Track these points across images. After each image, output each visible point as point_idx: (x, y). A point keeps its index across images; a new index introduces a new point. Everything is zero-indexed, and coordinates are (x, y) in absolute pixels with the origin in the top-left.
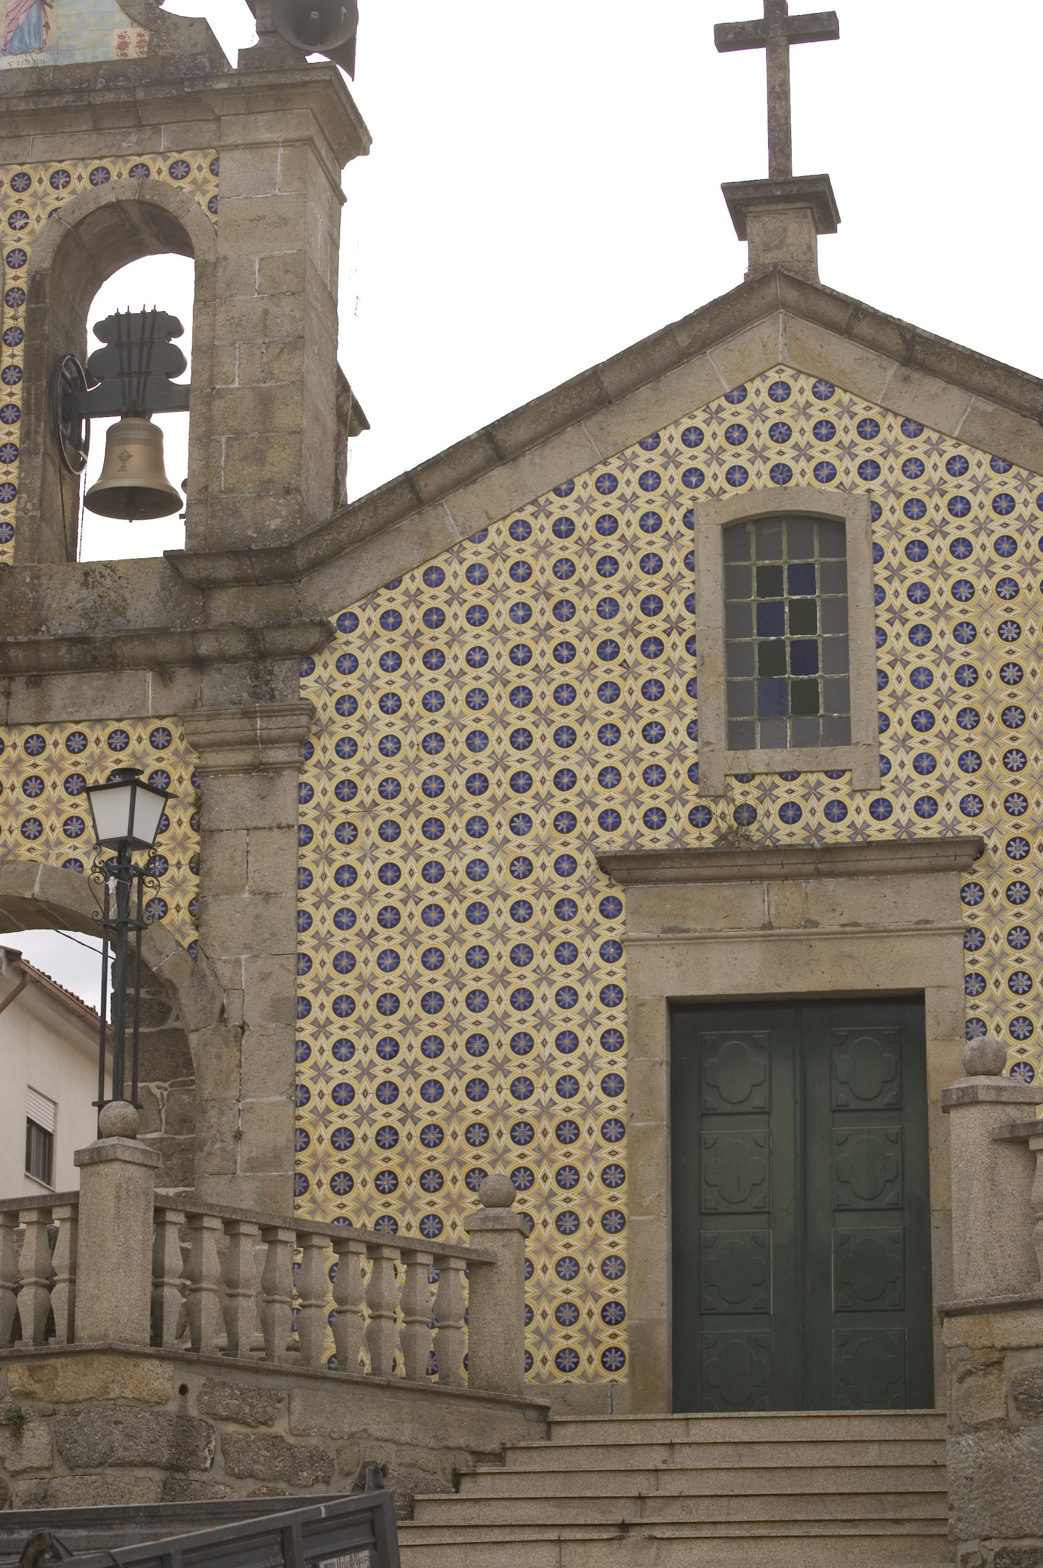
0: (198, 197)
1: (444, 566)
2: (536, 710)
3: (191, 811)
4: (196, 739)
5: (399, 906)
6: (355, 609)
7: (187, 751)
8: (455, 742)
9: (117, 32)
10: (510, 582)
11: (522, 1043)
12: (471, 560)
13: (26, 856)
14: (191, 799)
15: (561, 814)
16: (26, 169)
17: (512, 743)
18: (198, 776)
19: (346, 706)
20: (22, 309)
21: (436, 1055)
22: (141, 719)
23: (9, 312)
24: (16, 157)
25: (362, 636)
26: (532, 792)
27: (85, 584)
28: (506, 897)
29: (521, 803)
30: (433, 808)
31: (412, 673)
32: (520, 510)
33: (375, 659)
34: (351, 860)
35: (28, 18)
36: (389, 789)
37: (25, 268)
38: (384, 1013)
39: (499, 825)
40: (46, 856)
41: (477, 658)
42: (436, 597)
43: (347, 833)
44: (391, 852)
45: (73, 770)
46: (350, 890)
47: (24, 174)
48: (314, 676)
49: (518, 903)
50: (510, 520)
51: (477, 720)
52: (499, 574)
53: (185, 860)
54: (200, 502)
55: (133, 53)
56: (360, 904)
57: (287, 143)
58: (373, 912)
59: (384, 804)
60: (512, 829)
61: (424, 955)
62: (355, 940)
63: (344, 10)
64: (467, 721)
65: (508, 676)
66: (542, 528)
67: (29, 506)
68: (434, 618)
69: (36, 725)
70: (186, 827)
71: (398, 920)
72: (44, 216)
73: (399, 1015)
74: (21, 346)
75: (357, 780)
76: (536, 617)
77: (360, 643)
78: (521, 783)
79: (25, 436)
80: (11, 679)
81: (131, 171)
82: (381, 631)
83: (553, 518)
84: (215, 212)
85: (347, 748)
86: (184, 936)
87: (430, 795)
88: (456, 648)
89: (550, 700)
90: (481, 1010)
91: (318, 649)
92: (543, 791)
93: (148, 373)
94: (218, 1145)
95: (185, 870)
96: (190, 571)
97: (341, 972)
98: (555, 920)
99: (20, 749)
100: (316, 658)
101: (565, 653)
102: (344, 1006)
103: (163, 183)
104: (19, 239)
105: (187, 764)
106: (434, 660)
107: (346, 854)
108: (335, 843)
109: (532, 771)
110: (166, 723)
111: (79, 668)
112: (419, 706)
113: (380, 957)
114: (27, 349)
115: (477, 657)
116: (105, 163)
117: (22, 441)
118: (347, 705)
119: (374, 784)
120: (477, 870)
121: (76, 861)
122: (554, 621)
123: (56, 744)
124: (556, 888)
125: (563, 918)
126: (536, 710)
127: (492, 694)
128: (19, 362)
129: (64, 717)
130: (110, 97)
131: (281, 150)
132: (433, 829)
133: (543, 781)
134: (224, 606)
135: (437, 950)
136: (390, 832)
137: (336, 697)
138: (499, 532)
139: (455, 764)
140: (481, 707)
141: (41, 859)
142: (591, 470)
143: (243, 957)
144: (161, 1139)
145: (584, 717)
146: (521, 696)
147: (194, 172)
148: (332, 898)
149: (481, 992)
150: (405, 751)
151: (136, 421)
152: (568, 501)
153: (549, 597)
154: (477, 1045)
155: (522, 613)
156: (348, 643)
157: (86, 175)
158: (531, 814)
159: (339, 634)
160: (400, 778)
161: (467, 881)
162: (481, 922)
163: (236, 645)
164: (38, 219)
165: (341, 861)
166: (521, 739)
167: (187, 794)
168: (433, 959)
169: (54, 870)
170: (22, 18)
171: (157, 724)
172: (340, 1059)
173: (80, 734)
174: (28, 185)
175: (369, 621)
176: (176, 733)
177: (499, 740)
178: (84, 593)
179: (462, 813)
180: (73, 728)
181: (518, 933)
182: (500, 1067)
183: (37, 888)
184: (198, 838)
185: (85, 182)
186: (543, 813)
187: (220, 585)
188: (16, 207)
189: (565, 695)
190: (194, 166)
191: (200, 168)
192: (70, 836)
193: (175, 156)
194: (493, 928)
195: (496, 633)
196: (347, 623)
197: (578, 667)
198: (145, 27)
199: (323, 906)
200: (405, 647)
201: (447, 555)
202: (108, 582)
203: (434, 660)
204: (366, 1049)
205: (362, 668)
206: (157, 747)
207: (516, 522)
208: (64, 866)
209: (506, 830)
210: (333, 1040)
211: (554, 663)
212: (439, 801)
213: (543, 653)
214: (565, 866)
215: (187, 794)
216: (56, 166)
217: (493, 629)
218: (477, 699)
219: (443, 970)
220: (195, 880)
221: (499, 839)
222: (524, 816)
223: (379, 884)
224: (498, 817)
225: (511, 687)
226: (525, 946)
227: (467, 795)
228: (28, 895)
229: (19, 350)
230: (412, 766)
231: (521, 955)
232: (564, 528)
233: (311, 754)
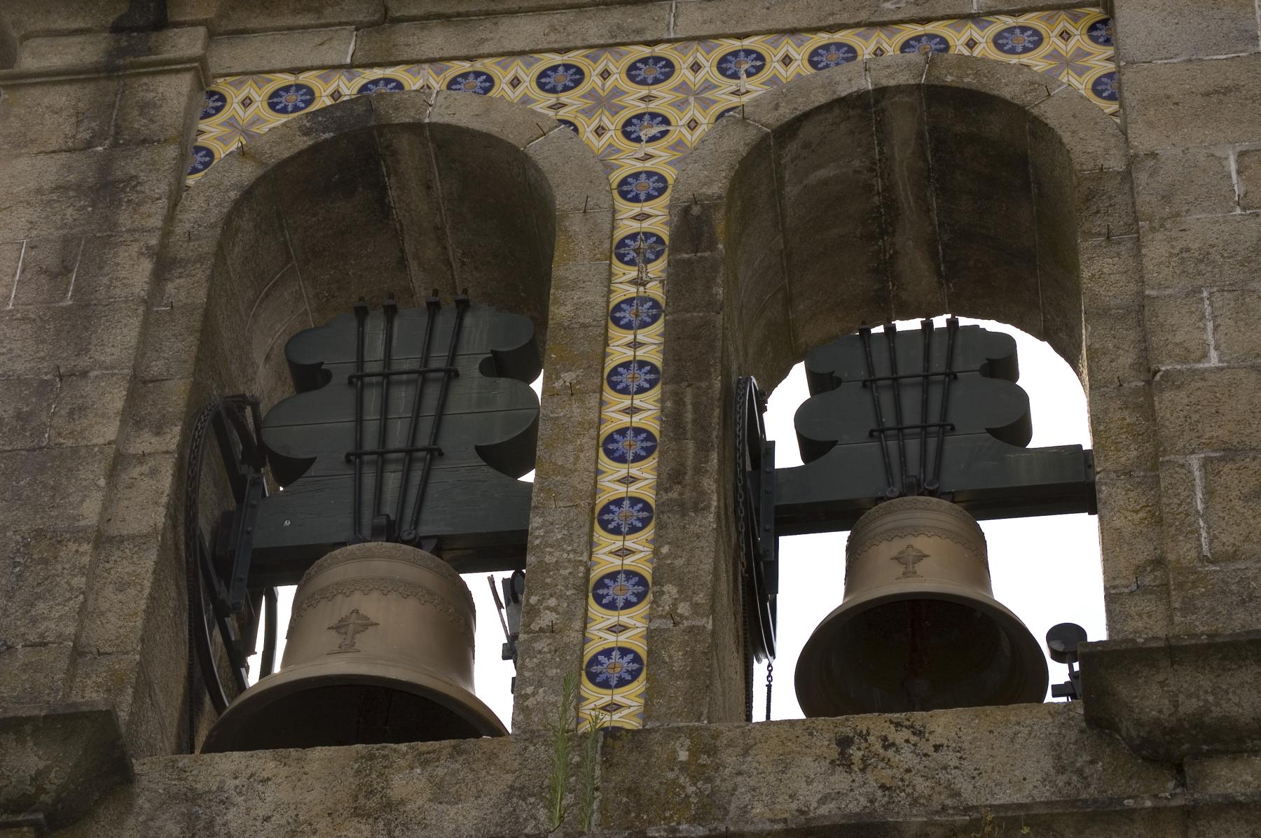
20: (657, 268)
37: (665, 199)
54: (1142, 590)
67: (683, 609)
74: (659, 326)
79: (670, 478)
93: (946, 428)
96: (1150, 699)
103: (984, 60)
178: (840, 780)
202: (906, 757)
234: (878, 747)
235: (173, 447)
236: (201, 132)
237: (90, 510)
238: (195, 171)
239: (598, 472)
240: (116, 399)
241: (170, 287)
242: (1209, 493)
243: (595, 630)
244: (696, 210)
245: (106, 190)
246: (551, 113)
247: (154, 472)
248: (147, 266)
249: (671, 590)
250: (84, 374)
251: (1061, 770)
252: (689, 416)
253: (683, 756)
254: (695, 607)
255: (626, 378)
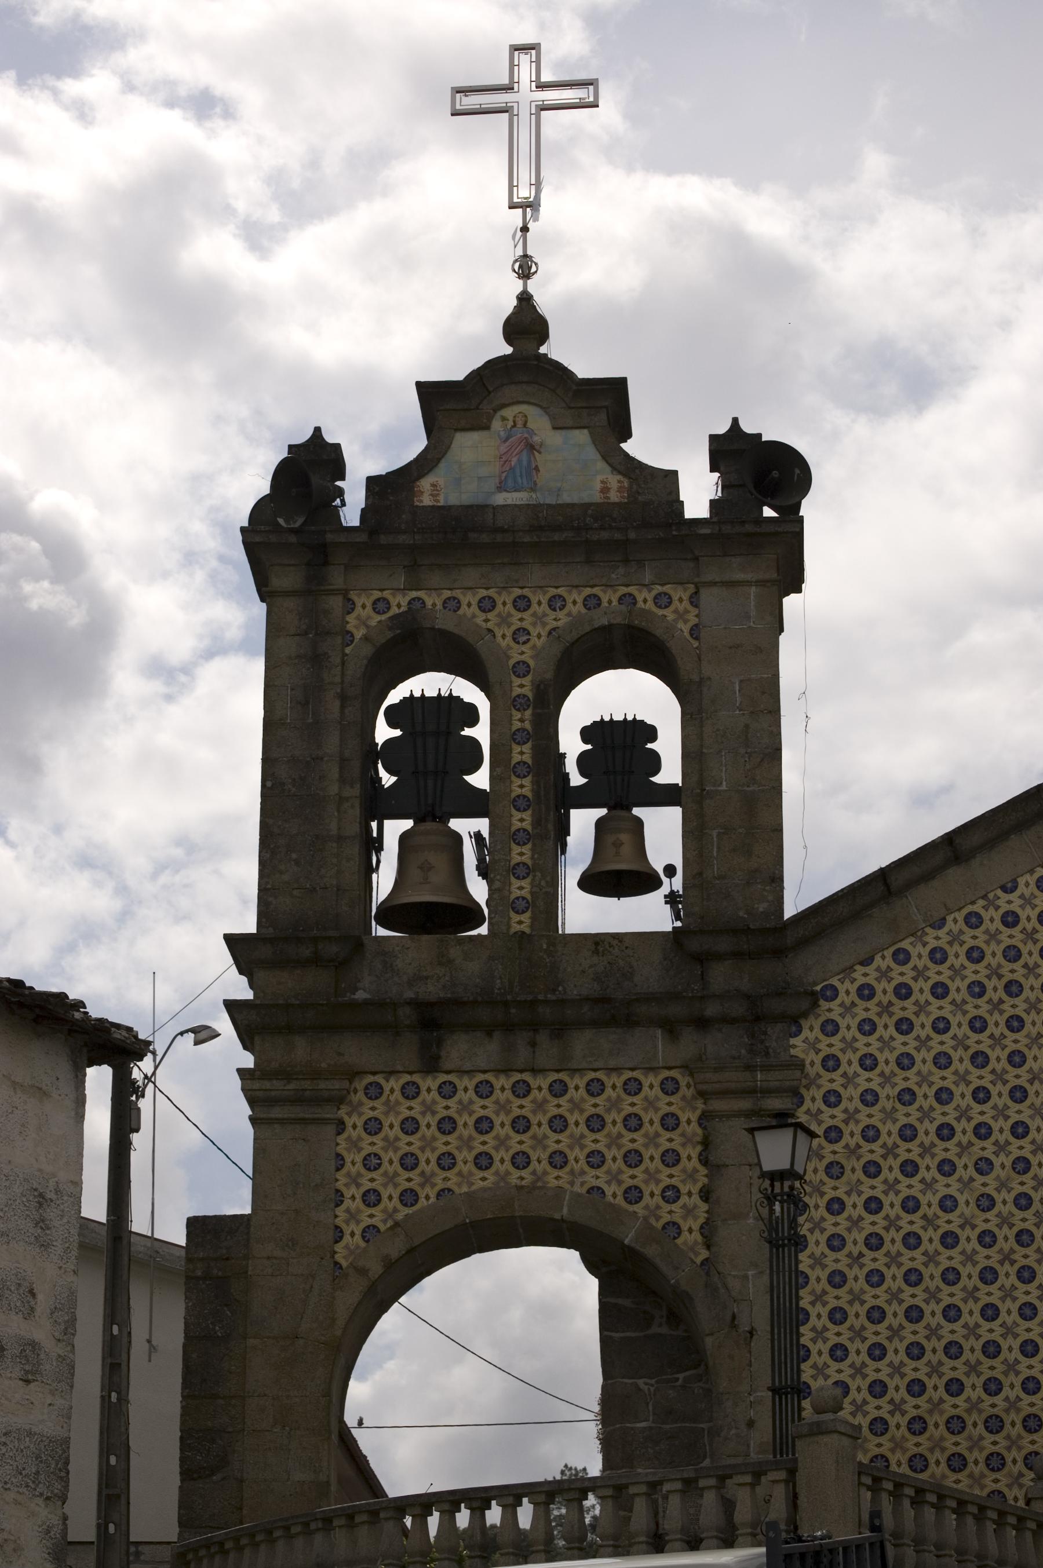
0: (680, 625)
1: (909, 948)
2: (993, 1071)
3: (699, 1148)
4: (704, 1087)
5: (882, 1232)
6: (835, 981)
7: (694, 1098)
8: (925, 1096)
9: (599, 478)
10: (967, 963)
11: (992, 1349)
12: (933, 944)
13: (553, 1183)
14: (699, 1139)
15: (1018, 1158)
16: (526, 592)
17: (974, 1098)
18: (705, 1118)
19: (831, 1063)
20: (528, 713)
21: (919, 1358)
22: (651, 1069)
23: (517, 715)
24: (517, 581)
25: (842, 1004)
26: (992, 1139)
27: (596, 952)
28: (973, 1227)
29: (983, 1149)
30: (909, 1151)
31: (886, 1037)
32: (973, 903)
33: (854, 1024)
34: (840, 1193)
35: (520, 461)
36: (871, 1134)
37: (529, 678)
38: (873, 1322)
39: (966, 1167)
40: (572, 1183)
41: (941, 1026)
42: (903, 974)
43: (835, 1170)
44: (874, 1188)
45: (593, 1111)
46: (839, 1219)
47: (525, 597)
48: (802, 1037)
49: (984, 1232)
50: (965, 911)
51: (944, 1078)
52: (957, 956)
53: (695, 1189)
55: (614, 497)
56: (849, 1230)
57: (761, 583)
58: (861, 1238)
59: (866, 1146)
60: (977, 1170)
61: (905, 1274)
62: (846, 1261)
63: (797, 471)
64: (935, 1078)
65: (968, 1042)
66: (992, 919)
67: (543, 883)
68: (903, 992)
69: (558, 1071)
70: (695, 1162)
71: (882, 1244)
72: (544, 633)
73: (886, 1324)
74: (529, 745)
75: (842, 1126)
76: (989, 993)
77: (841, 1010)
78: (982, 1131)
79: (537, 822)
80: (536, 1031)
81: (620, 599)
82: (857, 1001)
83: (1001, 911)
84: (697, 638)
85: (833, 1099)
86: (697, 1254)
87: (905, 1140)
88: (923, 1017)
89: (1004, 1063)
90: (955, 1321)
91: (805, 1015)
92: (1002, 1140)
94: (733, 1431)
95: (696, 1199)
97: (834, 1287)
98: (1016, 1247)
99: (545, 1091)
100: (802, 1022)
101: (1015, 1024)
102: (838, 1316)
104: (523, 653)
105: (694, 1109)
106: (904, 1027)
107: (835, 1188)
108: (826, 1179)
109: (991, 1122)
110: (673, 1073)
111: (596, 1024)
112: (893, 1065)
113: (867, 1276)
114: (533, 748)
115: (941, 1025)
116: (596, 590)
117: (533, 828)
118: (831, 1063)
119: (858, 1129)
120: (948, 1204)
121: (599, 1188)
122: (1005, 997)
123: (577, 1088)
124: (1015, 1220)
125: (1022, 1245)
126: (993, 1071)
127: (955, 1056)
128: (527, 758)
129: (584, 1065)
130: (605, 535)
131: (753, 589)
132: (909, 1168)
133: (1001, 1131)
134: (720, 976)
135: (916, 1270)
136: (872, 1170)
137: (821, 1055)
138: (955, 921)
139: (926, 1114)
140: (946, 1068)
141: (567, 1186)
142: (1032, 871)
143: (750, 1273)
144: (651, 1428)
145: (1034, 1079)
146: (980, 1059)
147: (676, 603)
148: (824, 1225)
149: (955, 1306)
150: (883, 1102)
151: (623, 813)
152: (1013, 897)
153: (1000, 977)
154: (953, 1350)
155: (978, 990)
156: (830, 1010)
157: (580, 600)
158: (993, 1158)
159: (822, 1002)
160: (879, 1125)
161: (940, 1213)
162: (953, 1247)
163: (738, 1009)
164: (539, 636)
165: (830, 1194)
166: (981, 1095)
167: (695, 1134)
168: (913, 1278)
169: (579, 1195)
170: (514, 461)
171: (667, 1073)
172: (836, 1360)
173: (598, 1080)
174: (529, 606)
175: (848, 993)
176: (683, 1083)
177: (963, 1096)
179: (933, 1156)
180: (592, 1075)
181: (985, 1258)
182: (973, 1369)
183: (565, 1211)
184: (706, 1172)
185: (580, 607)
186: (1002, 1157)
187: (719, 957)
188: (519, 625)
189: (1017, 1059)
190: (675, 598)
191: (681, 600)
192: (592, 1167)
193: (658, 589)
194: (963, 1252)
195: (956, 1005)
196: (828, 993)
197: (1028, 1036)
198: (624, 475)
199: (817, 1231)
200: (880, 1015)
201: (911, 939)
202: (616, 951)
203: (904, 1027)
204: (858, 1352)
205: (843, 1031)
206: (667, 1093)
207: (970, 914)
208: (588, 1192)
209: (971, 1171)
210: (830, 1344)
211: (1007, 1032)
212: (913, 1145)
213: (997, 1023)
214: (1023, 1202)
215: (695, 1134)
216: (553, 591)
217: (953, 1002)
218: (943, 1061)
219: (922, 1286)
220: (704, 1207)
221: (966, 1178)
222: (987, 1159)
223: (864, 1214)
224: (965, 1159)
225: (971, 1052)
226: (991, 1268)
227: (937, 1141)
228: (557, 1216)
229: (527, 748)
230: (889, 1115)
231: (988, 1276)
232: (1010, 920)
233: (802, 1103)
234: (607, 946)
235: (358, 794)
236: (348, 623)
237: (333, 827)
238: (348, 645)
239: (512, 816)
240: (334, 773)
241: (346, 711)
242: (719, 848)
243: (514, 888)
244: (542, 687)
245: (316, 659)
246: (484, 624)
247: (353, 807)
248: (337, 703)
249: (538, 874)
250: (322, 759)
251: (665, 959)
252: (542, 793)
253: (545, 946)
254: (547, 882)
255: (519, 770)
